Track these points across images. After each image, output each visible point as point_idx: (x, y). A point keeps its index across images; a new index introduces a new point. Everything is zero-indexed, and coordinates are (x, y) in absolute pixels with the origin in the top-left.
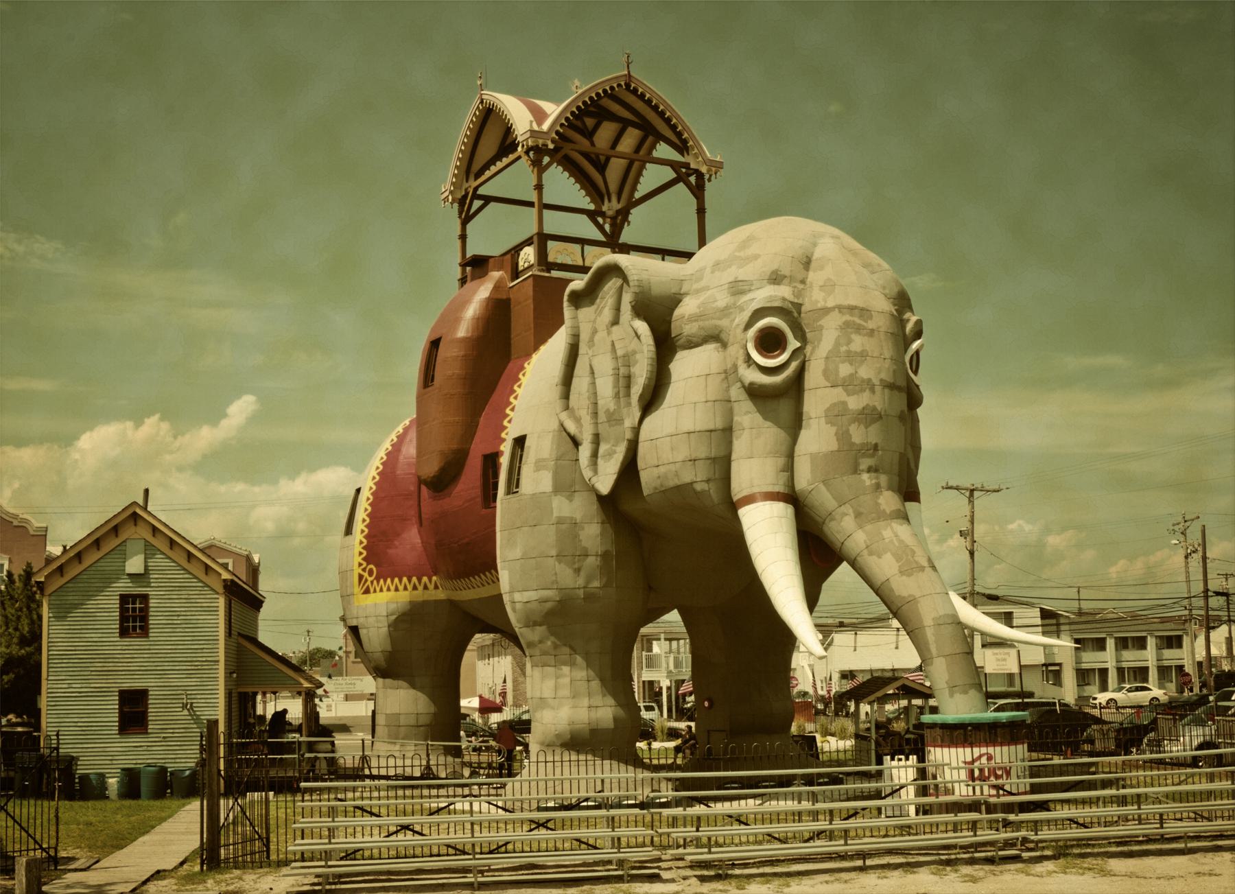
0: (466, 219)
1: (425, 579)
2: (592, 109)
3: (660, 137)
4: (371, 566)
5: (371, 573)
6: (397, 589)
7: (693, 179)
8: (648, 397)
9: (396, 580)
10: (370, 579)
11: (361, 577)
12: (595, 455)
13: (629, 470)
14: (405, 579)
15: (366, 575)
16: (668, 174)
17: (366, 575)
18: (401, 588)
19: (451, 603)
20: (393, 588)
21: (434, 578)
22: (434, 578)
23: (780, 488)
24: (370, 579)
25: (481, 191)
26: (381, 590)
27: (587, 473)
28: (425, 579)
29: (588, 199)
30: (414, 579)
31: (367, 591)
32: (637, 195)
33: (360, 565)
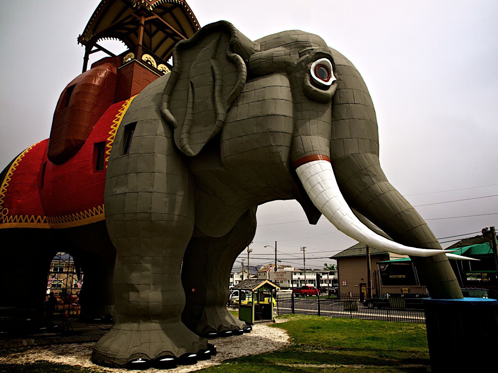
0: (88, 52)
1: (39, 217)
10: (3, 215)
18: (23, 221)
20: (18, 221)
21: (45, 217)
22: (45, 217)
24: (3, 215)
25: (98, 43)
28: (39, 217)
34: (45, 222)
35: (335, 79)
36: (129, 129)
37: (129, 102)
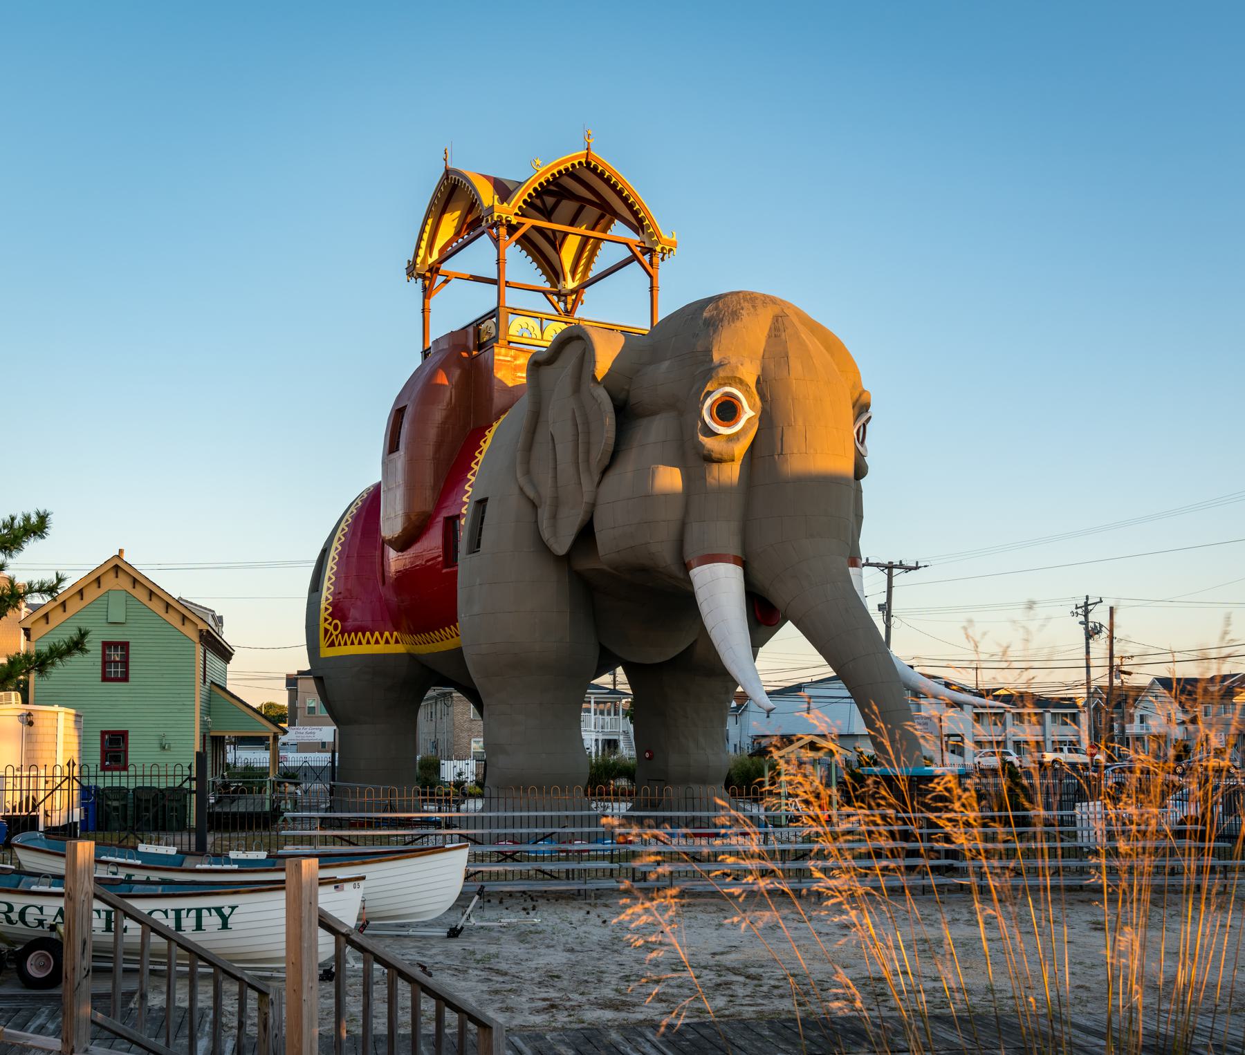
1: (387, 634)
2: (552, 188)
3: (616, 215)
4: (336, 621)
5: (336, 627)
6: (360, 643)
7: (647, 257)
8: (606, 462)
9: (360, 634)
10: (335, 633)
11: (326, 631)
12: (554, 517)
13: (586, 534)
14: (368, 634)
15: (331, 628)
16: (625, 253)
17: (331, 628)
18: (364, 642)
19: (411, 656)
21: (395, 633)
22: (395, 633)
23: (738, 553)
24: (335, 633)
26: (346, 644)
27: (546, 535)
28: (387, 634)
29: (544, 278)
30: (377, 634)
31: (332, 644)
32: (591, 275)
33: (326, 620)
34: (397, 642)
35: (752, 414)
36: (481, 503)
37: (490, 435)
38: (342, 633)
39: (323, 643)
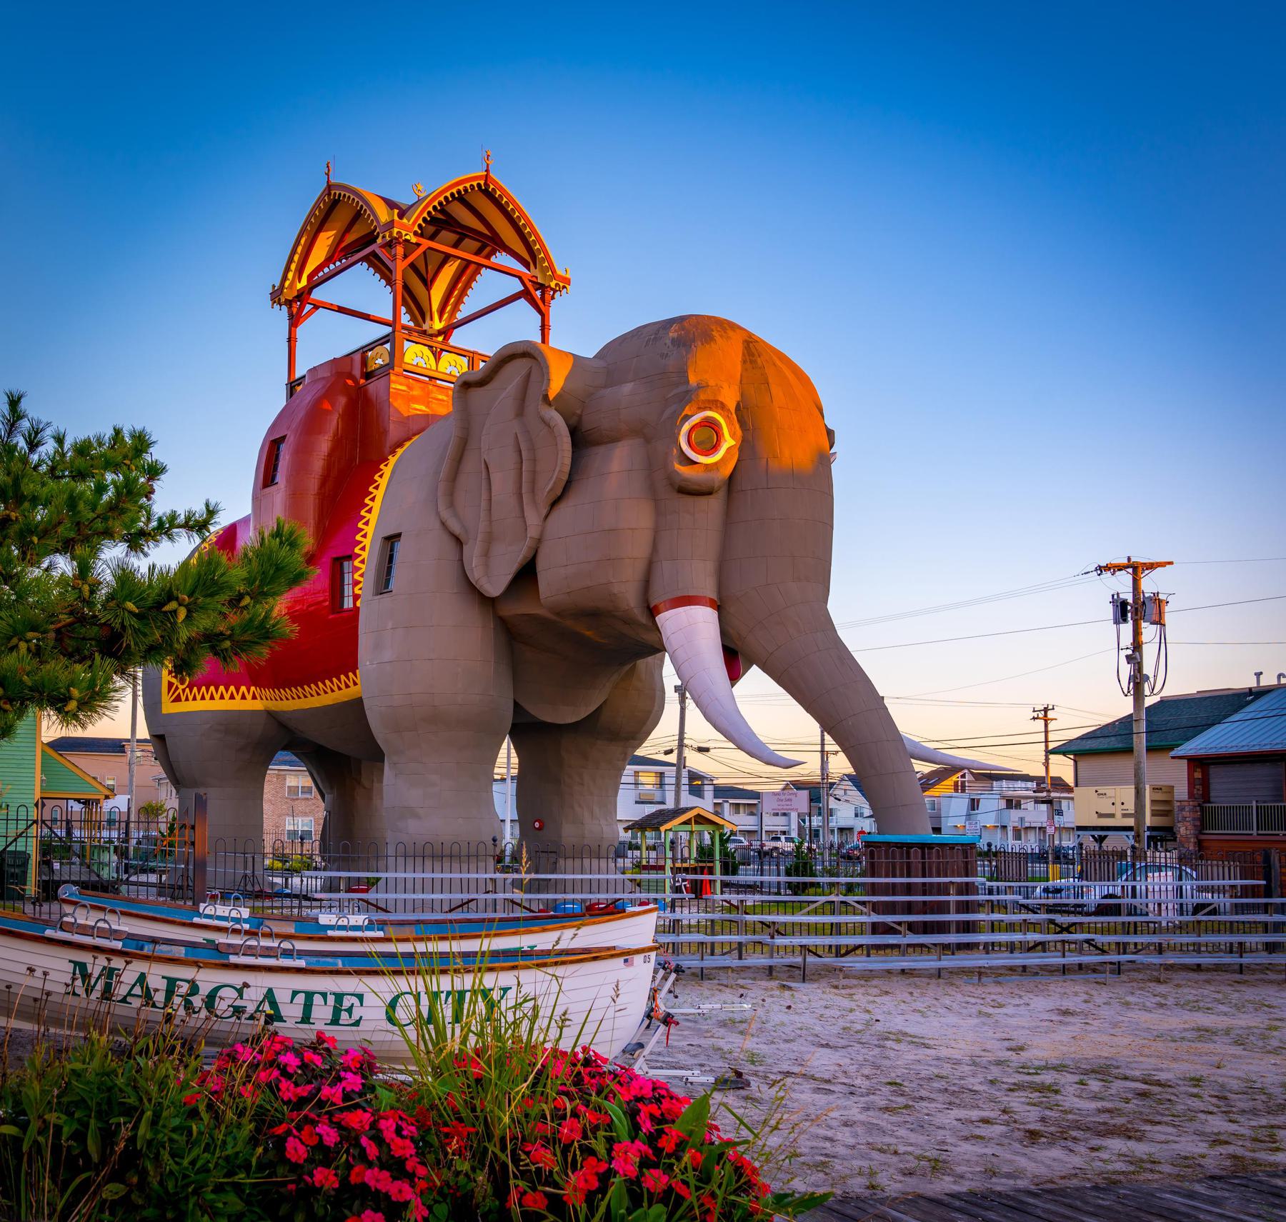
7: (538, 293)
9: (212, 688)
10: (181, 687)
11: (170, 685)
13: (527, 575)
16: (517, 287)
22: (253, 688)
31: (178, 699)
38: (191, 687)
39: (166, 698)
